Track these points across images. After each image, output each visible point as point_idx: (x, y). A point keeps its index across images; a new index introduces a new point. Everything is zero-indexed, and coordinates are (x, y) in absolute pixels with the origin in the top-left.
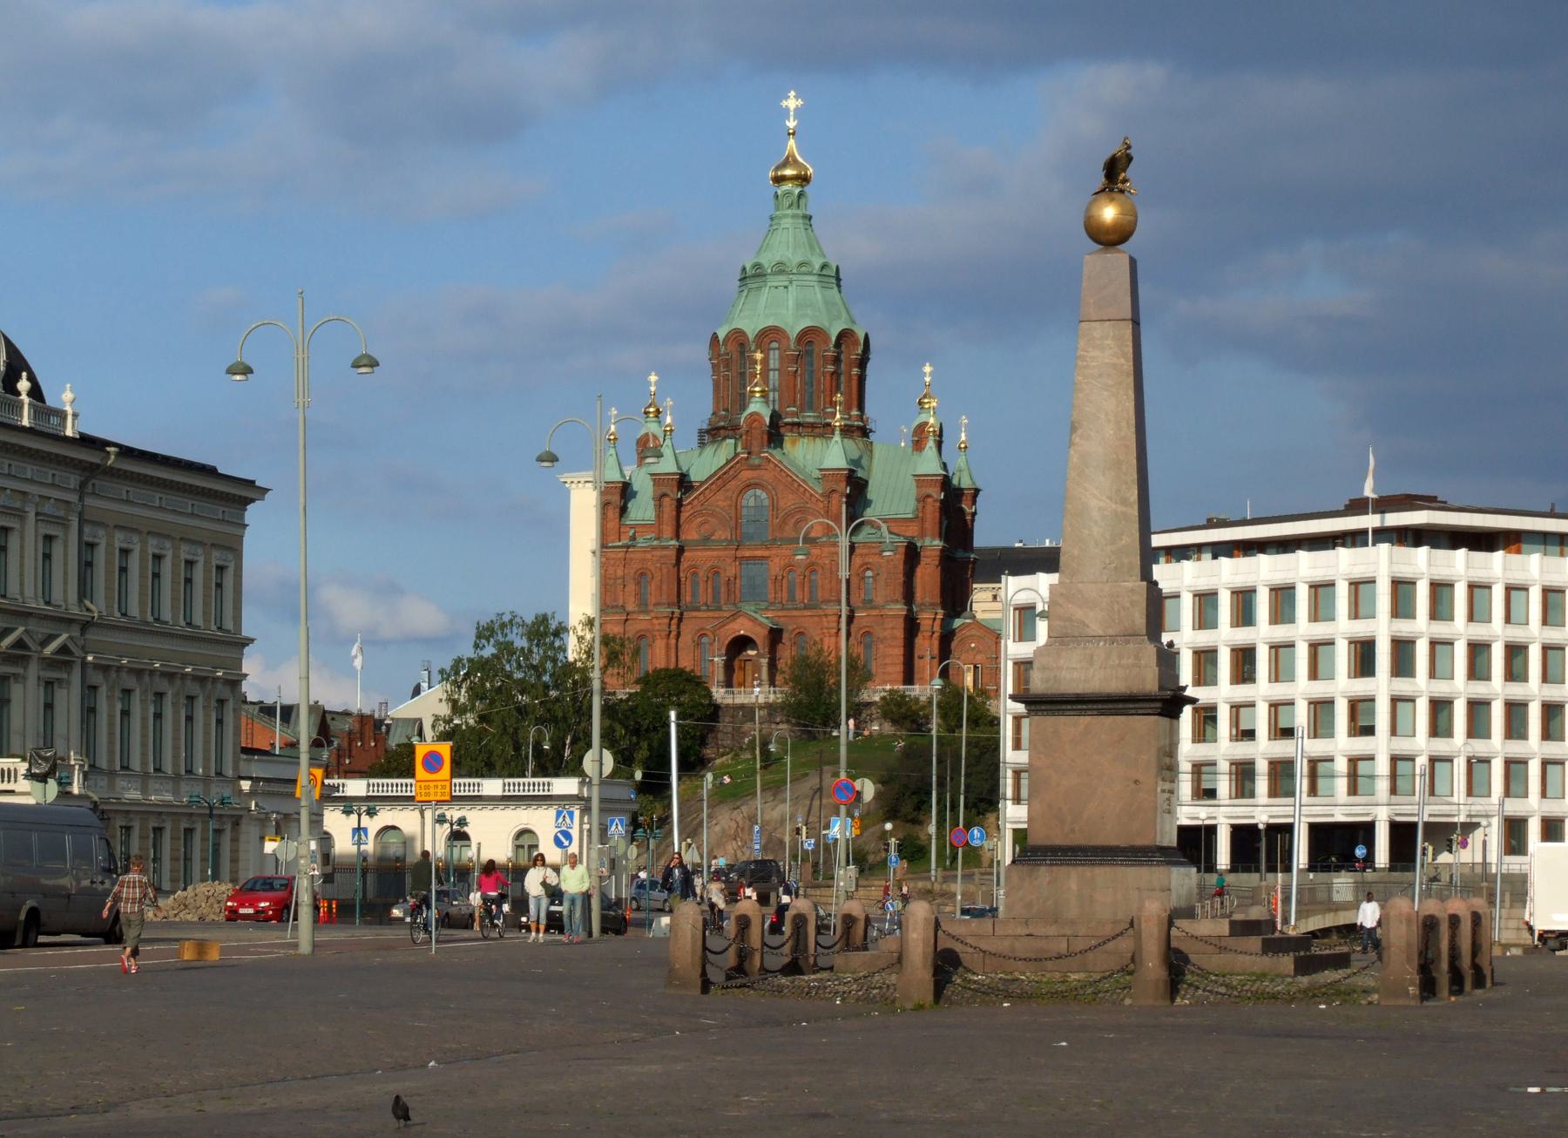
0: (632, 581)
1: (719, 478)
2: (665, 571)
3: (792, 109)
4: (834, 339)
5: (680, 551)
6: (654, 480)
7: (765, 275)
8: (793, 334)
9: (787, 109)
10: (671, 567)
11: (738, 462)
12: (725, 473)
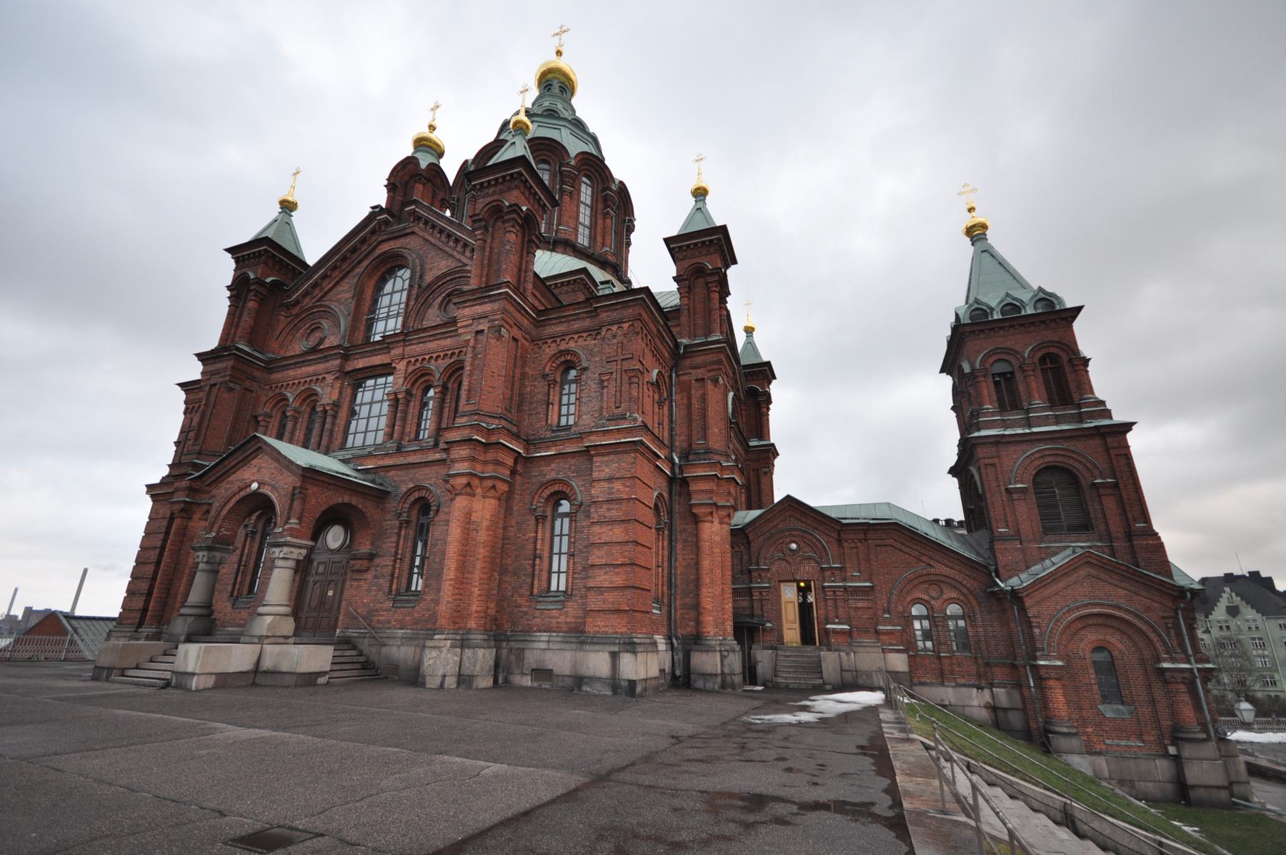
1: (344, 259)
6: (237, 262)
11: (373, 232)
12: (354, 250)
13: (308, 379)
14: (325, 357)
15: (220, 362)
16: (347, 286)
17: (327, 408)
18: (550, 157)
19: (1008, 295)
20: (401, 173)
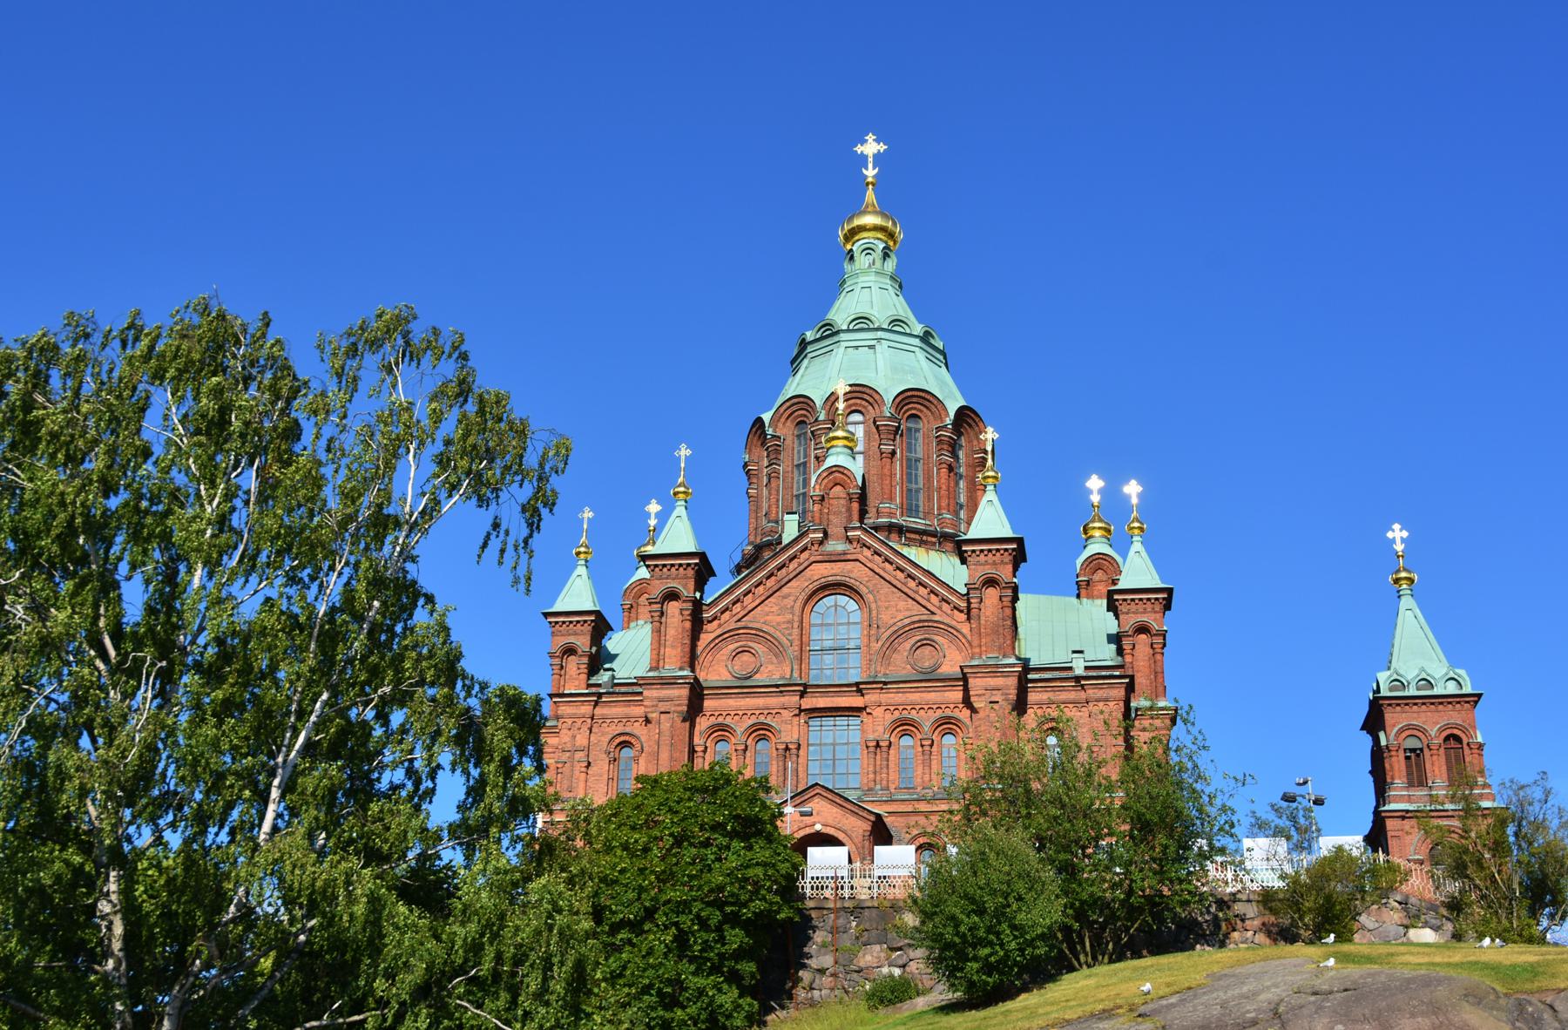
0: (604, 756)
2: (666, 725)
3: (871, 155)
4: (952, 414)
5: (697, 694)
7: (838, 332)
8: (889, 397)
9: (864, 158)
10: (678, 721)
11: (805, 549)
13: (757, 712)
14: (781, 692)
15: (667, 689)
16: (775, 609)
17: (790, 746)
18: (921, 411)
19: (1423, 670)
20: (826, 481)
